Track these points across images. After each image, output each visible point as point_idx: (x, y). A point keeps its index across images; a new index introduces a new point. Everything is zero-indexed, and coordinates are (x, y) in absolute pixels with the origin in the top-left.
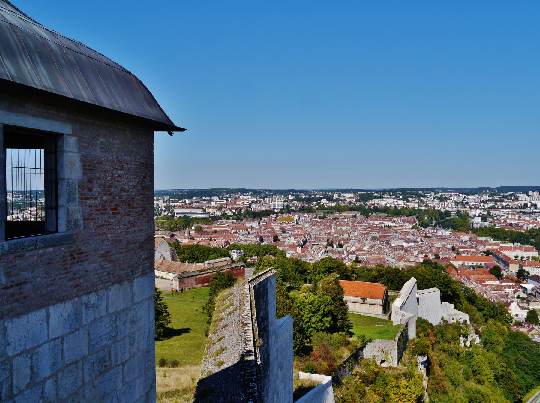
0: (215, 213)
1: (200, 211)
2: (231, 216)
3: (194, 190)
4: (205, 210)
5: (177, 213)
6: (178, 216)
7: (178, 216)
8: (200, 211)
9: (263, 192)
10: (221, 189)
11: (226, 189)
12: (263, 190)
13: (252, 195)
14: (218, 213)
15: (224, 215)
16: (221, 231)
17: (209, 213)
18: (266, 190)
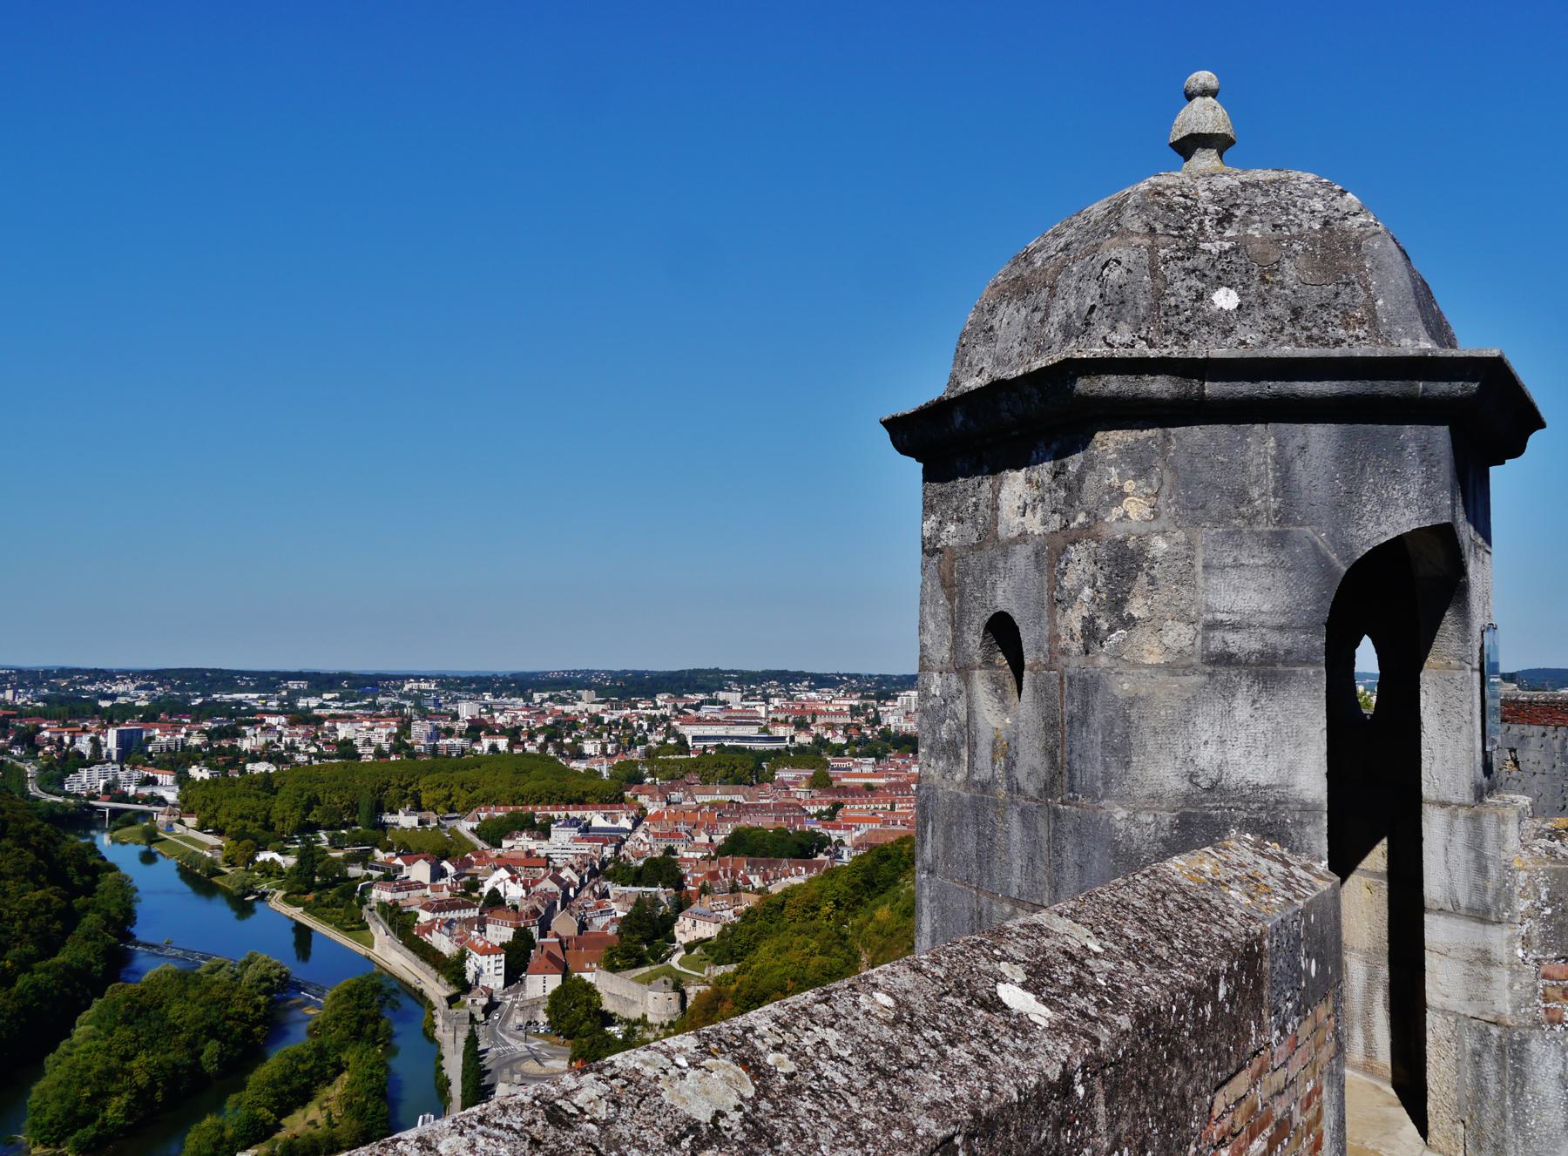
0: (792, 739)
1: (753, 731)
2: (846, 747)
3: (642, 673)
4: (765, 730)
5: (695, 738)
6: (700, 745)
7: (700, 745)
8: (753, 731)
9: (843, 682)
10: (717, 671)
11: (734, 672)
12: (841, 676)
13: (811, 688)
14: (804, 739)
15: (820, 742)
16: (890, 785)
17: (783, 739)
18: (851, 676)
